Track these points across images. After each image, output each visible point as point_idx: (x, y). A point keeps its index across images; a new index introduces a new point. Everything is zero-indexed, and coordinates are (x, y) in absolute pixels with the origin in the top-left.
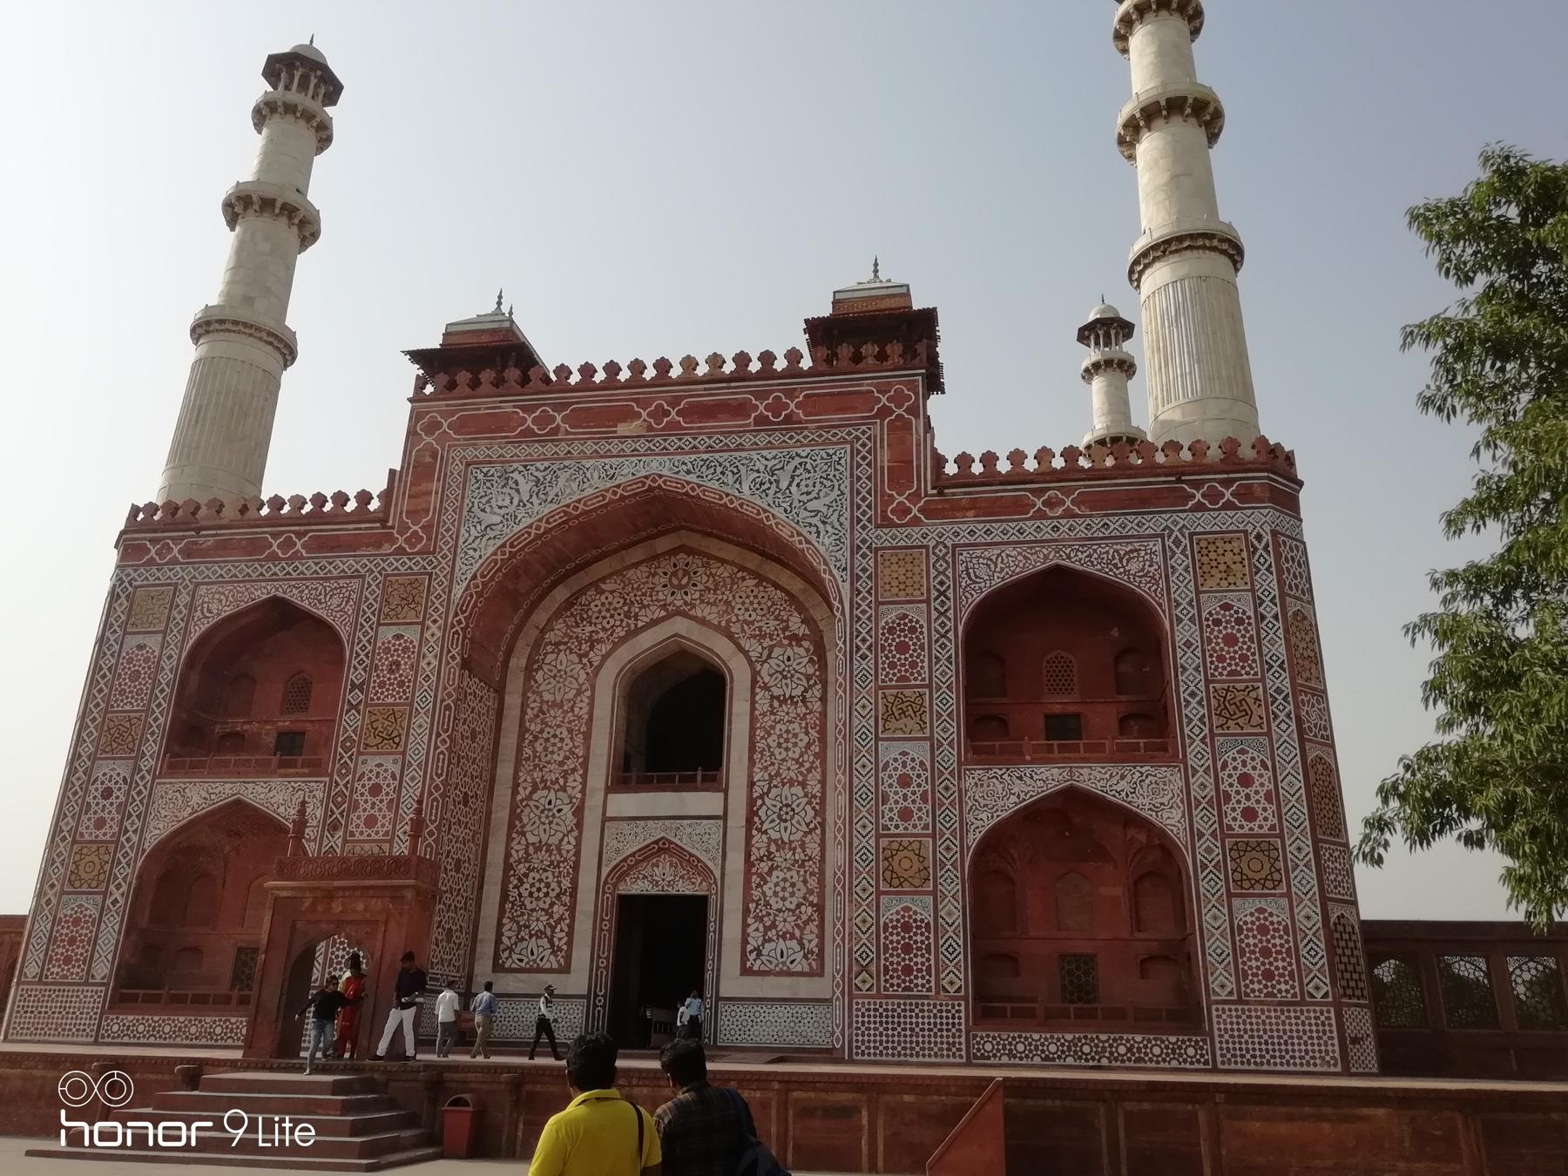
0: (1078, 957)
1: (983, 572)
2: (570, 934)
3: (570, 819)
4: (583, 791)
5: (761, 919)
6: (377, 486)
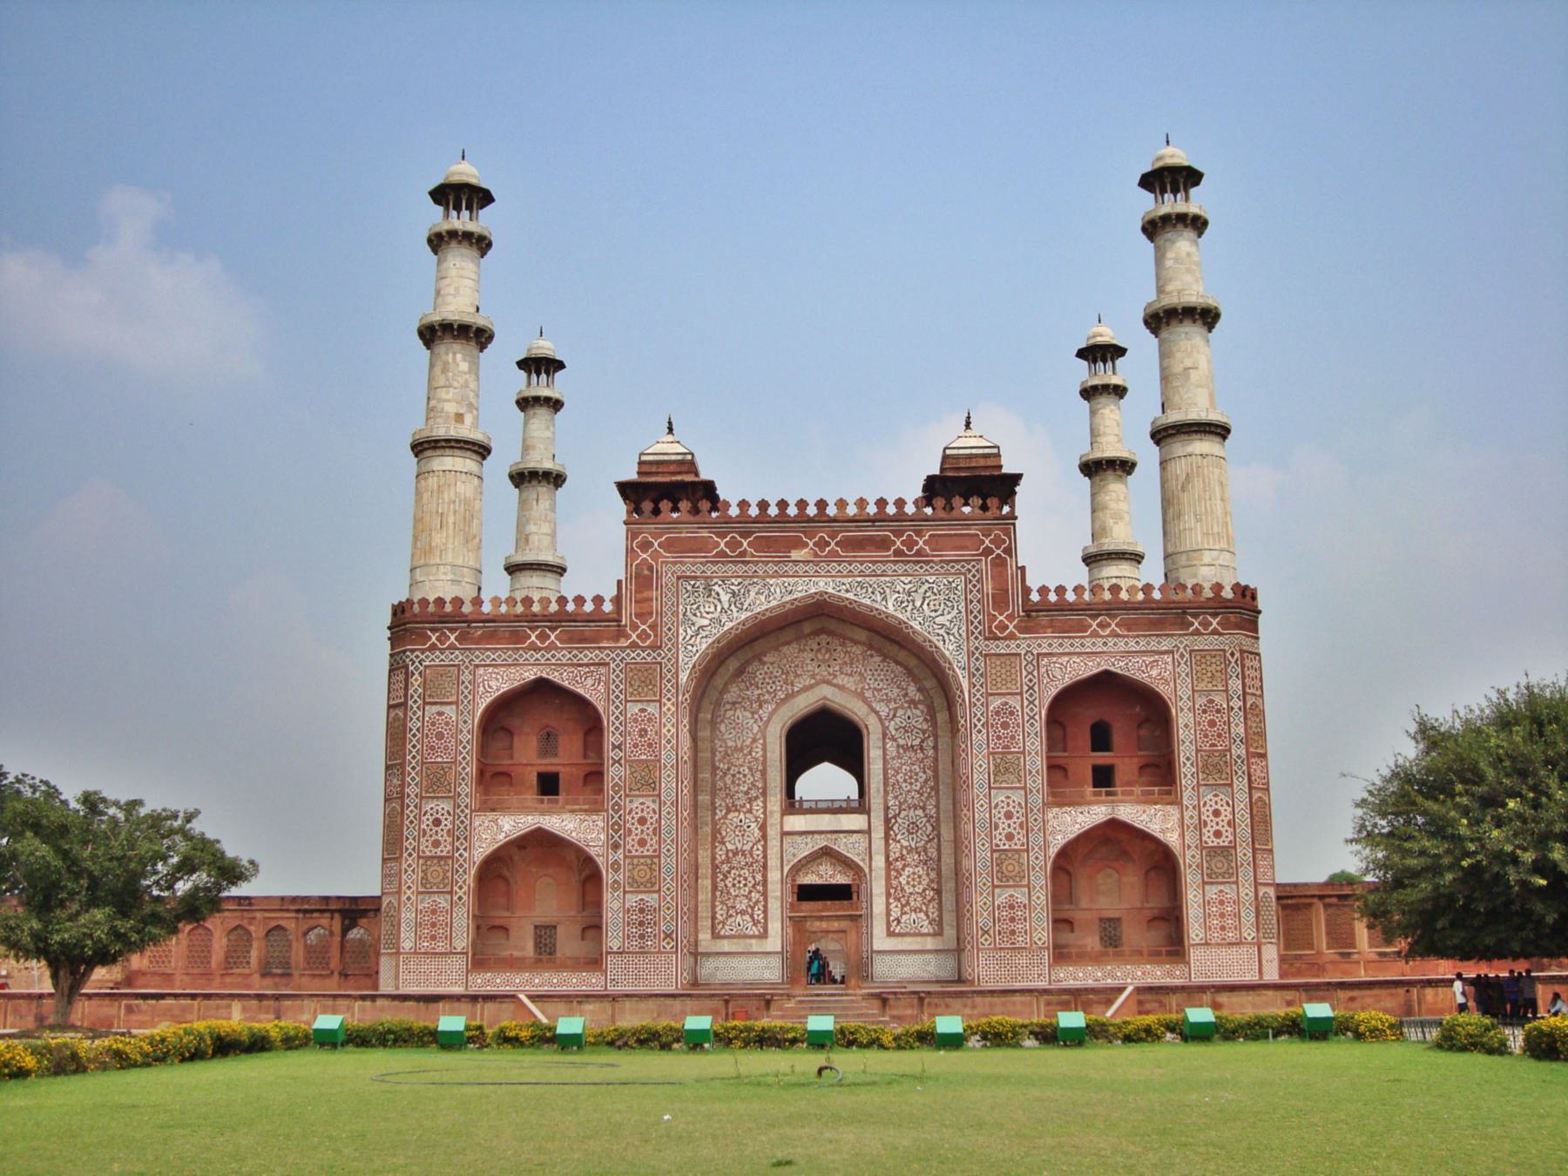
0: (1110, 920)
1: (1058, 674)
2: (765, 912)
3: (757, 833)
4: (764, 813)
5: (899, 900)
6: (609, 592)
